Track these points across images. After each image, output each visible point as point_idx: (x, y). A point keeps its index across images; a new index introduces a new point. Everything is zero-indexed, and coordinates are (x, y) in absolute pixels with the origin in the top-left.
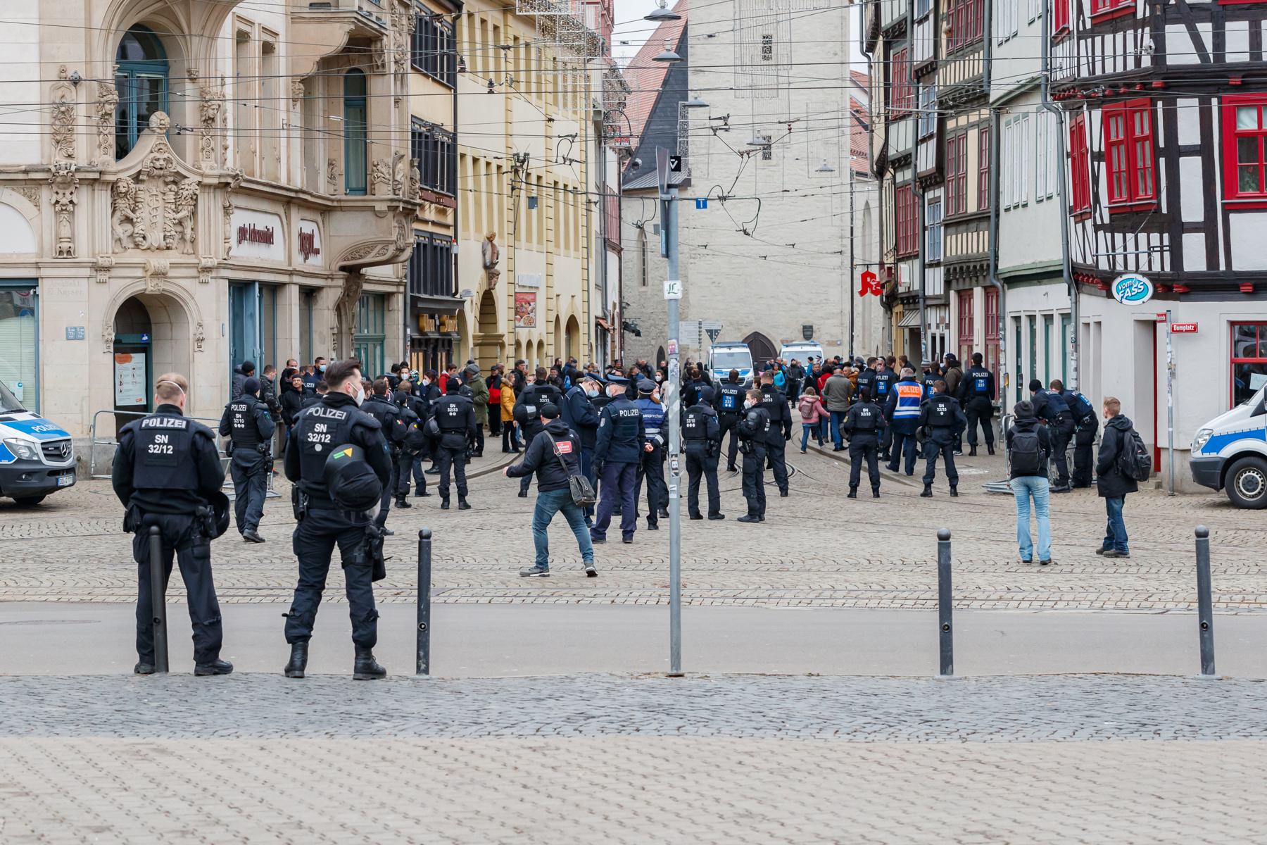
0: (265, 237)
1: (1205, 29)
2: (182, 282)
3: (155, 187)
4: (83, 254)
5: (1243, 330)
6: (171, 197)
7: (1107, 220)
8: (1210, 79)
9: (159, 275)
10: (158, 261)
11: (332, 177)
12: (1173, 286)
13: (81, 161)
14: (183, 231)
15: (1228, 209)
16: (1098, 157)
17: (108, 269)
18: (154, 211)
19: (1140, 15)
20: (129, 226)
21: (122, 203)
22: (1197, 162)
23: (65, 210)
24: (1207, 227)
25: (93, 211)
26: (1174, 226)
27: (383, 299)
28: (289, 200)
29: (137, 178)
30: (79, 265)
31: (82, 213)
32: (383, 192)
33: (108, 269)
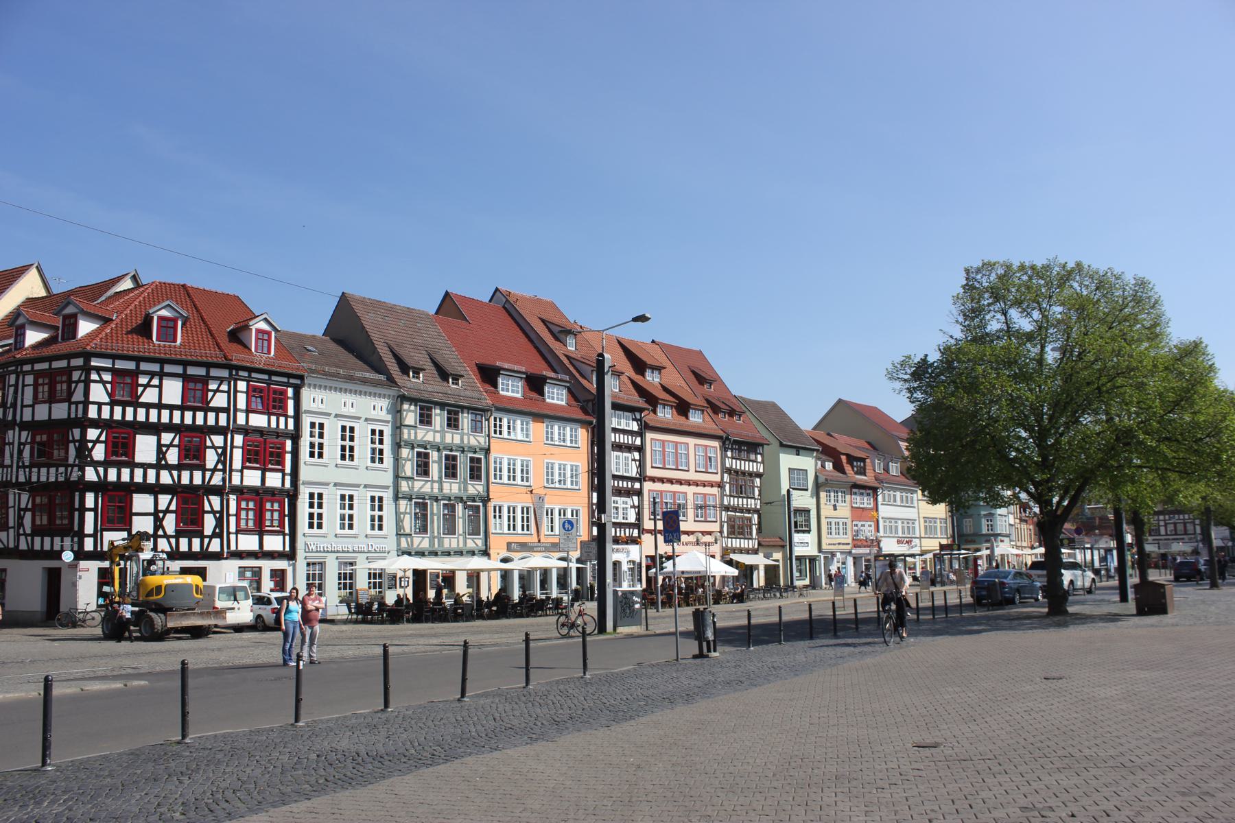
1: (101, 470)
5: (100, 569)
7: (28, 531)
8: (101, 487)
12: (81, 555)
15: (103, 530)
16: (26, 510)
19: (71, 460)
22: (92, 513)
24: (94, 535)
26: (81, 535)
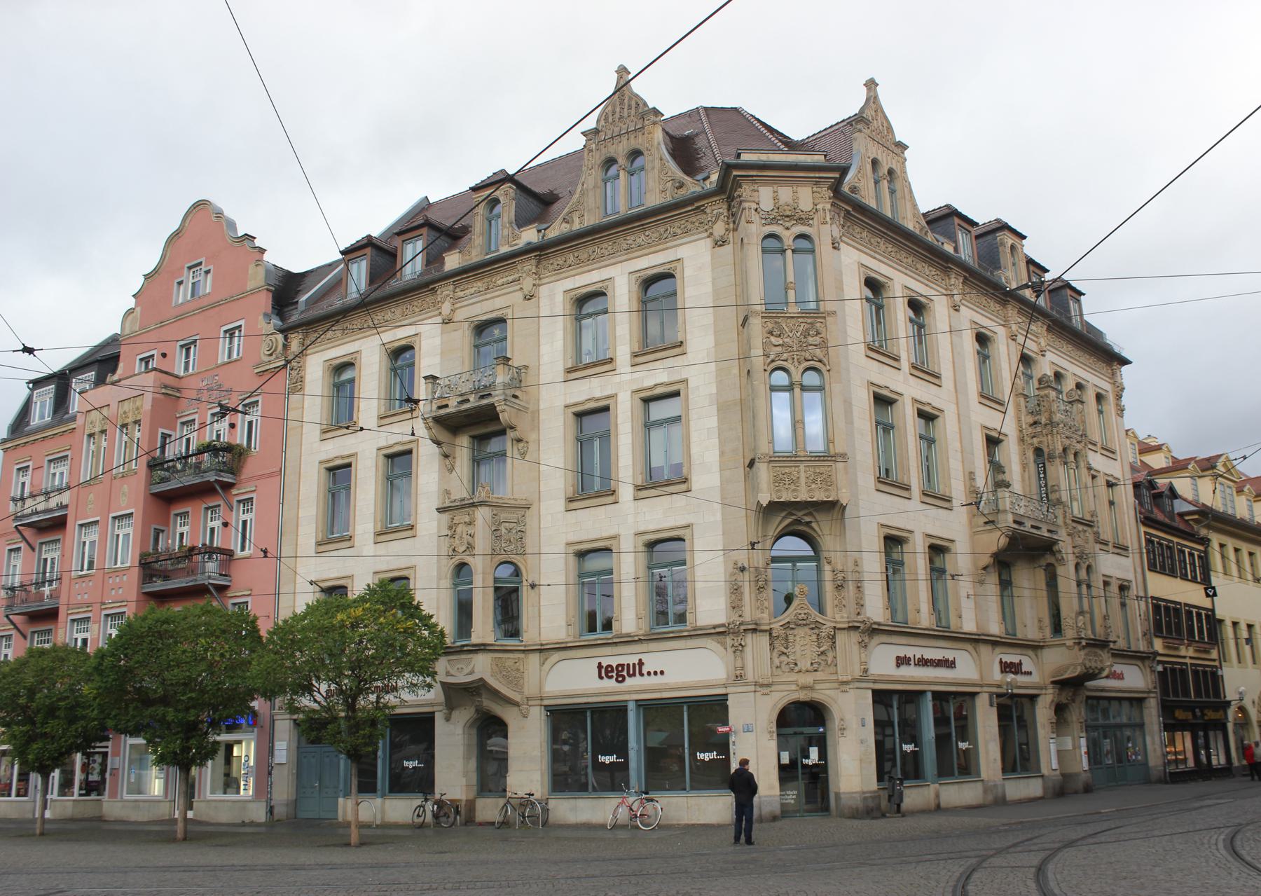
0: (949, 664)
2: (827, 692)
3: (800, 632)
4: (750, 677)
6: (814, 637)
9: (811, 688)
10: (807, 679)
11: (1041, 628)
13: (747, 618)
14: (825, 657)
17: (768, 685)
18: (804, 647)
20: (784, 658)
21: (777, 643)
23: (739, 649)
25: (757, 646)
27: (1137, 701)
28: (975, 641)
29: (786, 626)
30: (747, 684)
31: (748, 650)
32: (1069, 633)
33: (768, 685)
